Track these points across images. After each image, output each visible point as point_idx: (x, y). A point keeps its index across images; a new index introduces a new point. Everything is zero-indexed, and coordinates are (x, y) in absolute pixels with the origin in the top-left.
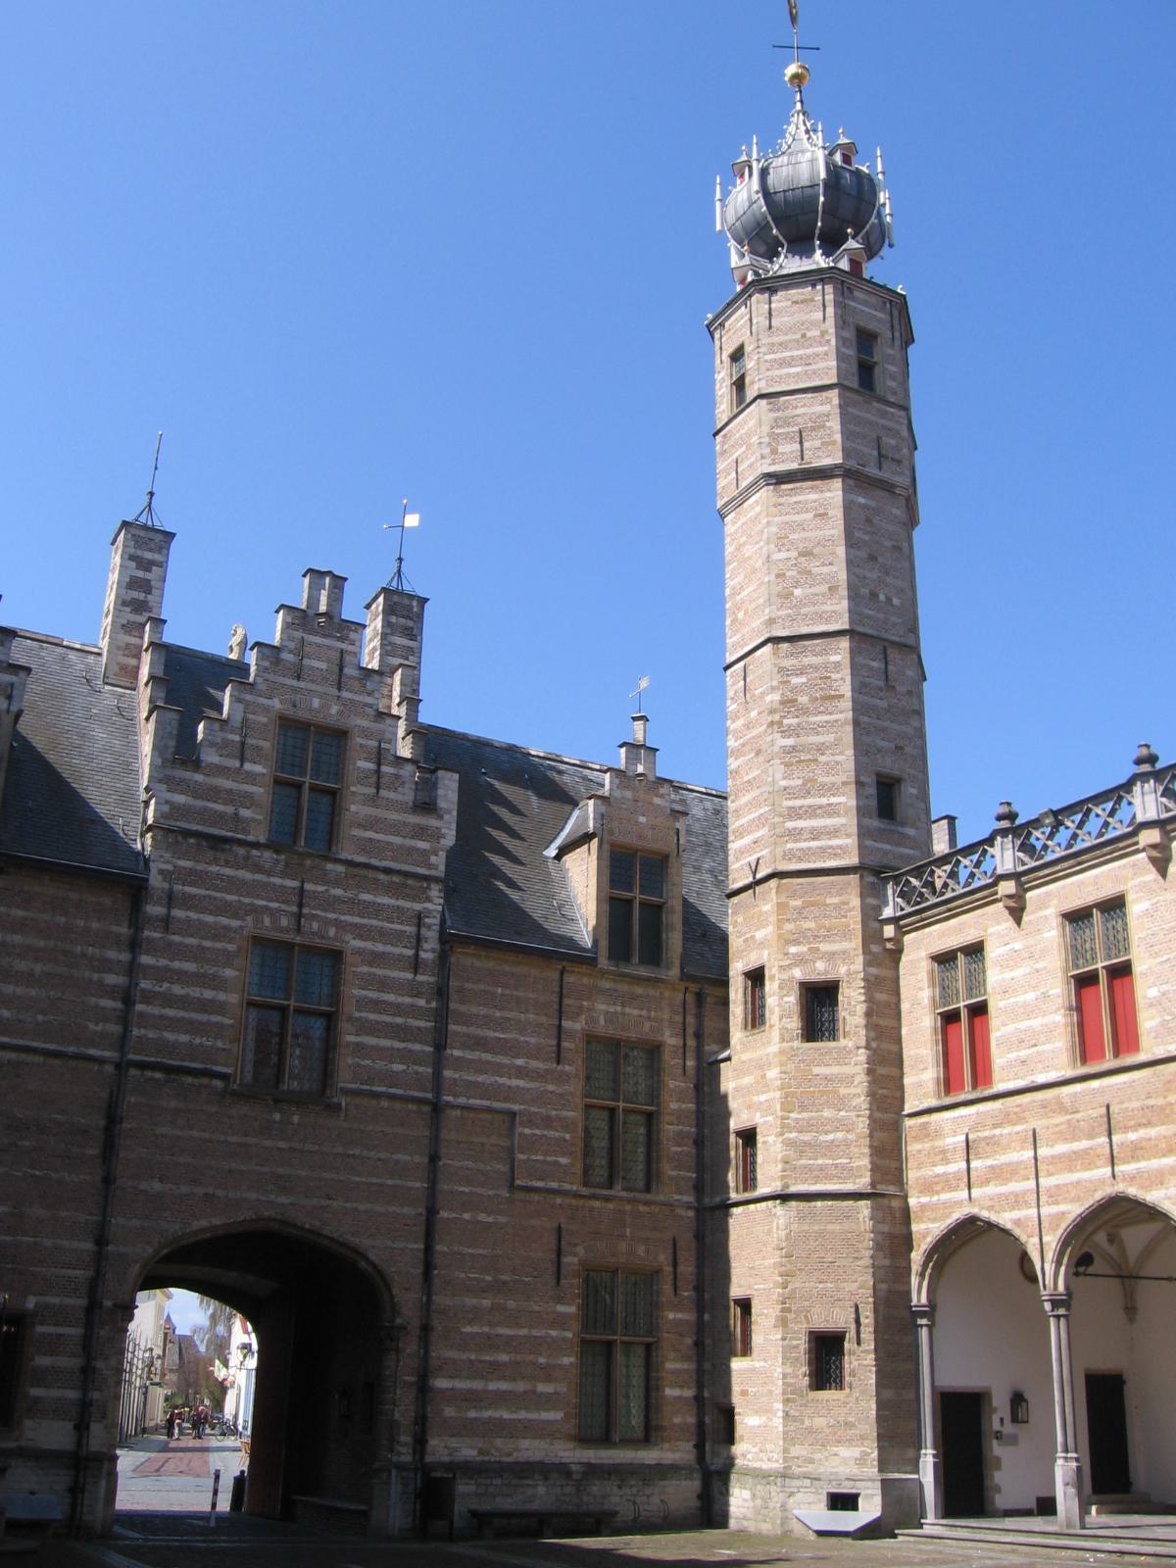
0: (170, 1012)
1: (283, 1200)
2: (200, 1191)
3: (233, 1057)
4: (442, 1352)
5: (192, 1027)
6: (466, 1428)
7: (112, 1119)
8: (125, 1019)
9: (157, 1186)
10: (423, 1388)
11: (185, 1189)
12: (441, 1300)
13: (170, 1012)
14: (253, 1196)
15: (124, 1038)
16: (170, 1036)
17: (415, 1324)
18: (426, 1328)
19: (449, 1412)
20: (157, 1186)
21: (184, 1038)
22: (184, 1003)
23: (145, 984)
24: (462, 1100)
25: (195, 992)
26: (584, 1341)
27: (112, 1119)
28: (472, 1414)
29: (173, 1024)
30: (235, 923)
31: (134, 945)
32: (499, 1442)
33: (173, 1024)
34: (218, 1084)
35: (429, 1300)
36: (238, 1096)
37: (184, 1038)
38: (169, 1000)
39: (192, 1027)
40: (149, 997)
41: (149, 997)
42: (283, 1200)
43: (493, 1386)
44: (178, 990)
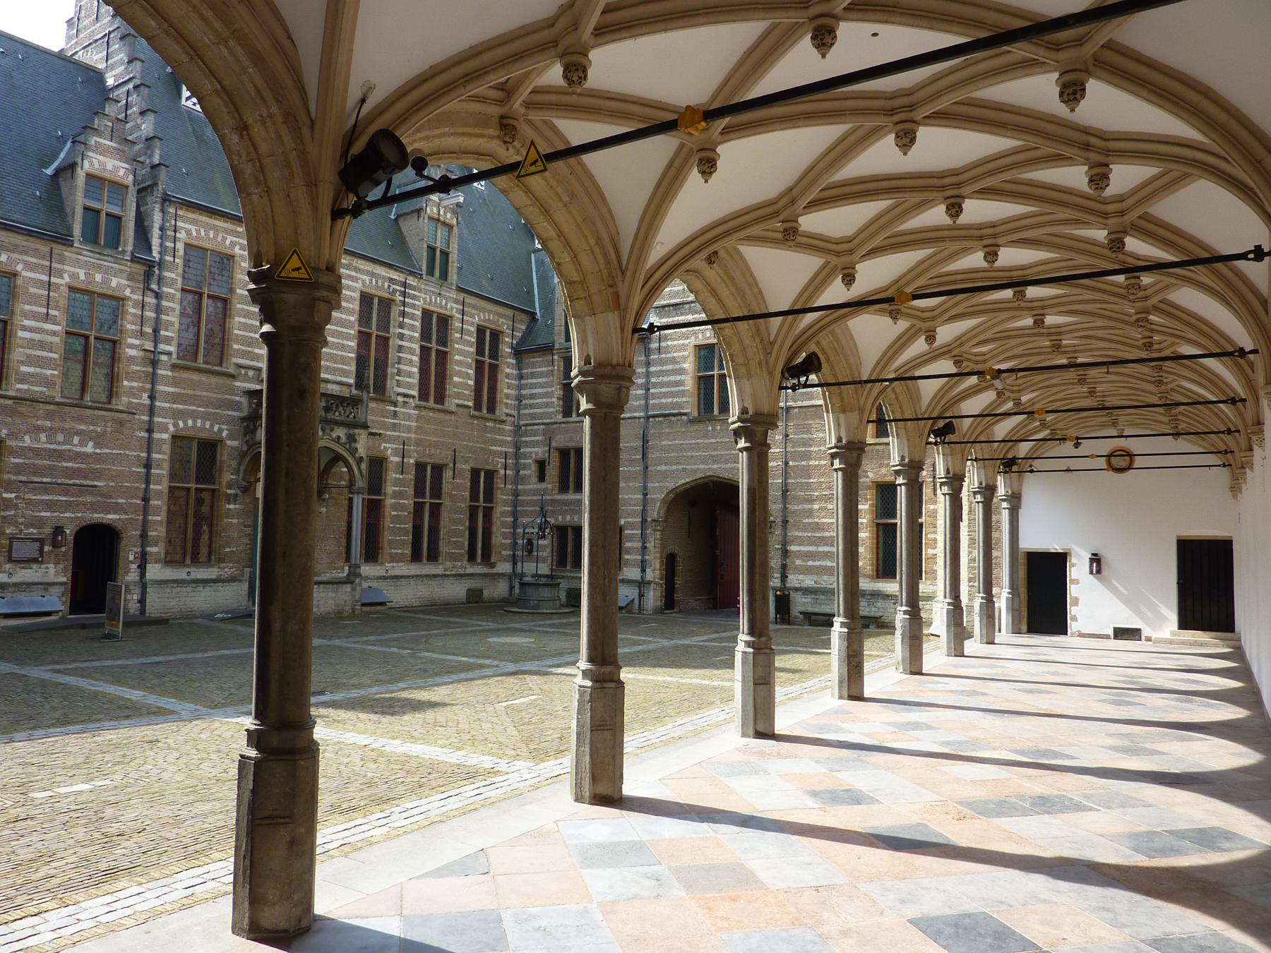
0: (663, 390)
1: (715, 466)
2: (680, 467)
3: (689, 404)
4: (793, 533)
5: (673, 395)
6: (808, 571)
7: (645, 441)
8: (646, 398)
9: (664, 468)
10: (785, 553)
11: (675, 467)
12: (792, 507)
13: (663, 390)
14: (702, 466)
15: (647, 405)
16: (664, 401)
17: (779, 520)
18: (785, 522)
19: (798, 562)
20: (664, 468)
21: (670, 400)
22: (668, 384)
23: (653, 380)
24: (799, 404)
25: (672, 378)
26: (878, 524)
27: (645, 441)
28: (810, 563)
29: (665, 395)
30: (687, 342)
31: (648, 364)
32: (825, 578)
33: (665, 395)
34: (685, 418)
35: (786, 508)
36: (690, 421)
37: (670, 400)
38: (662, 385)
39: (673, 395)
40: (655, 385)
41: (655, 385)
42: (715, 466)
43: (821, 549)
44: (666, 379)
